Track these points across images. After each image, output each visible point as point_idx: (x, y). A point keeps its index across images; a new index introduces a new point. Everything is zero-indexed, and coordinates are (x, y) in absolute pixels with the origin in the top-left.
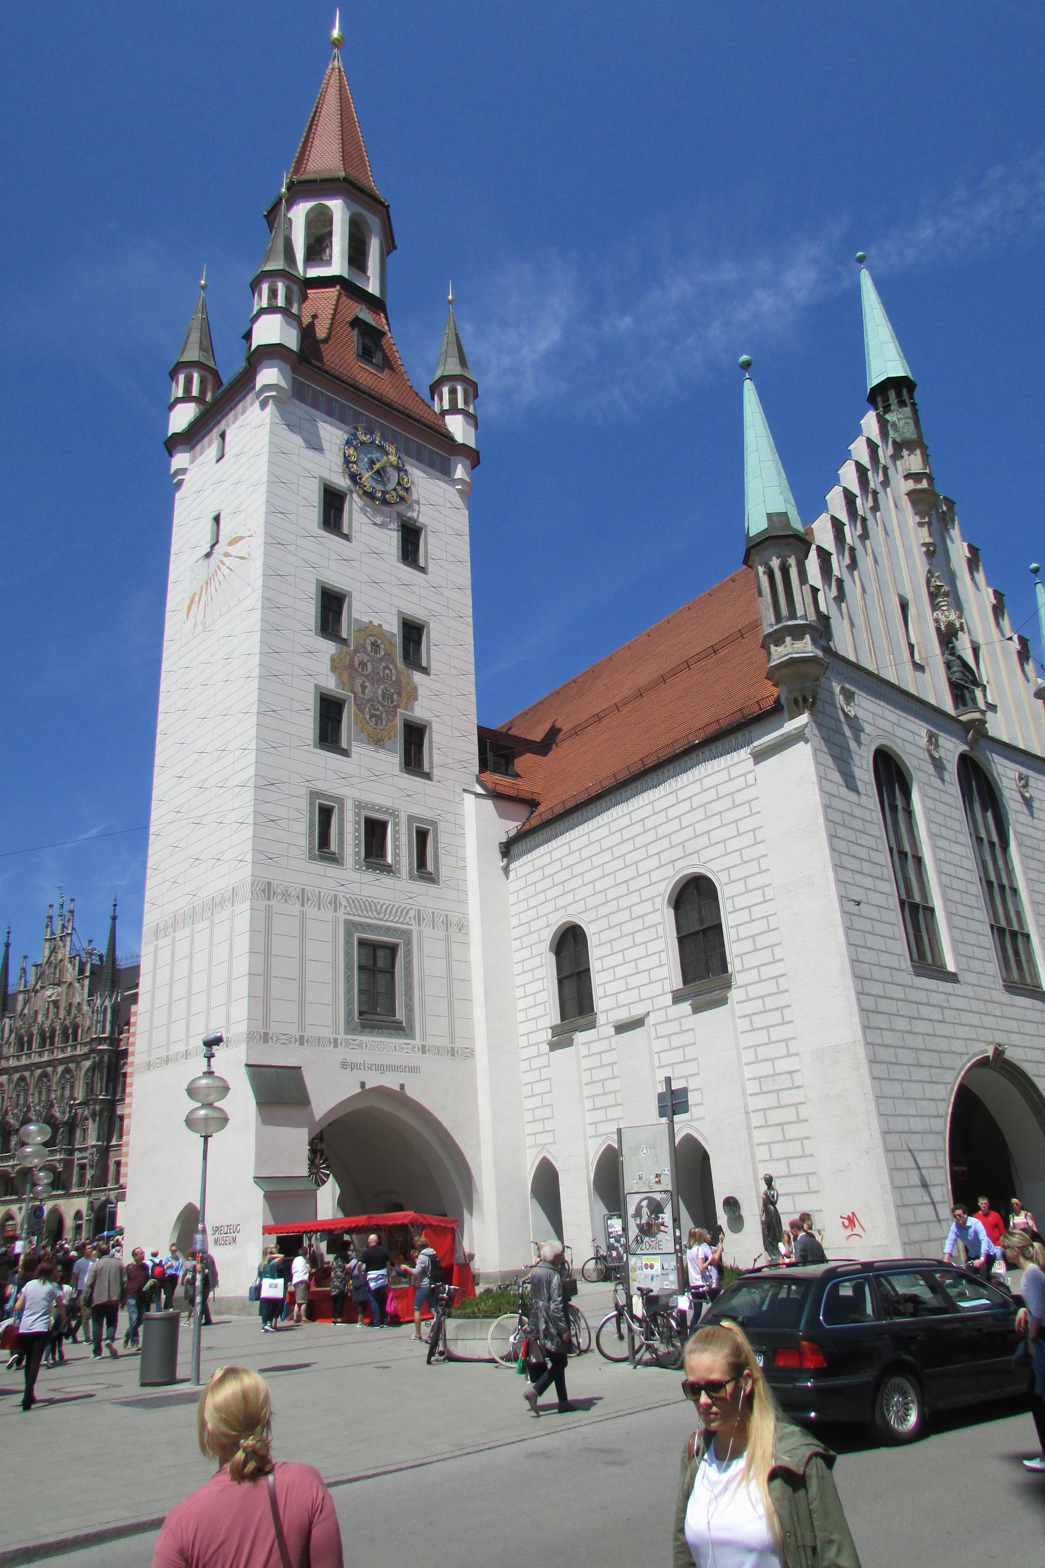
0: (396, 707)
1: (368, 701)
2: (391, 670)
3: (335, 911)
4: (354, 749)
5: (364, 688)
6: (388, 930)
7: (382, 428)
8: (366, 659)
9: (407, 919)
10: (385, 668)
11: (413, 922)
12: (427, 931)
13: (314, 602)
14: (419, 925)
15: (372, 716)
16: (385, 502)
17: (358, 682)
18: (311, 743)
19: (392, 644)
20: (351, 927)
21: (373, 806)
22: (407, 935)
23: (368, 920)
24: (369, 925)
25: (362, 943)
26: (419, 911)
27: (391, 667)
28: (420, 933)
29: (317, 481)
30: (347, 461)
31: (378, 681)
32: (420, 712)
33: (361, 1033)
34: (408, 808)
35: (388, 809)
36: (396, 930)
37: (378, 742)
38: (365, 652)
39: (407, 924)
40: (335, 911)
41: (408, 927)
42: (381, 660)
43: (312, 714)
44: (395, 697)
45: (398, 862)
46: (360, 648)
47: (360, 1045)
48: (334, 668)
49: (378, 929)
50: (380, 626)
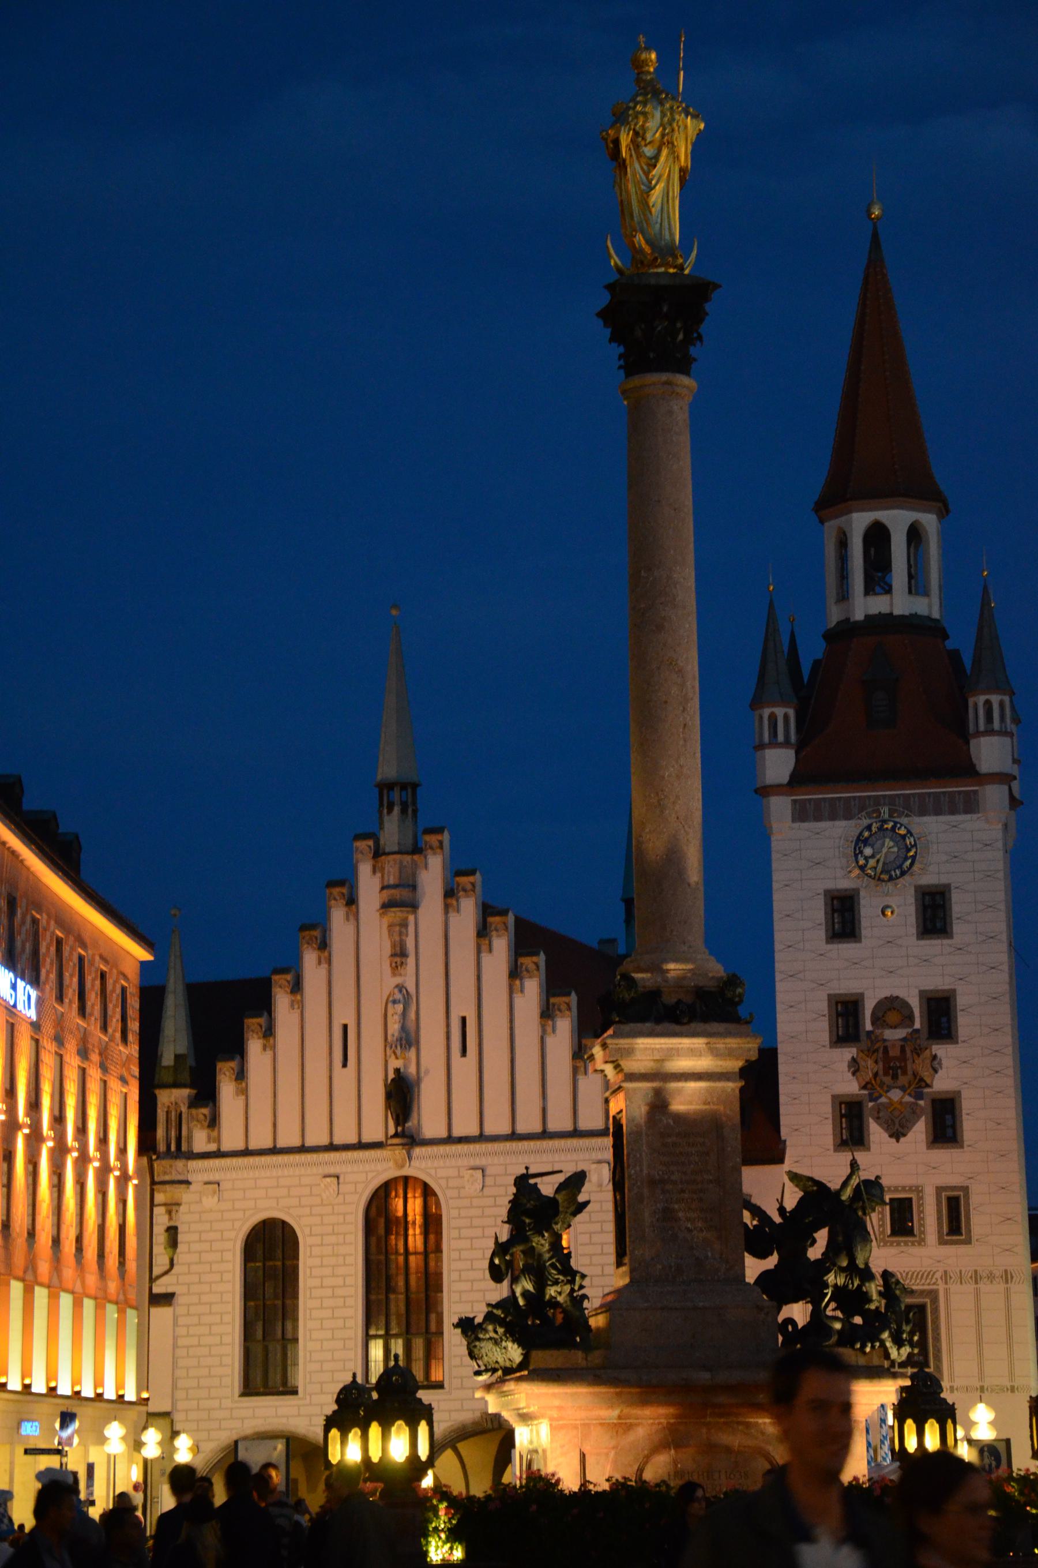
9: (934, 1280)
11: (940, 1281)
12: (954, 1287)
13: (827, 1018)
14: (946, 1283)
18: (832, 1147)
22: (933, 1295)
26: (946, 1272)
28: (947, 1291)
29: (822, 897)
32: (941, 1083)
35: (910, 1187)
39: (934, 1284)
41: (935, 1287)
43: (830, 1121)
45: (923, 1232)
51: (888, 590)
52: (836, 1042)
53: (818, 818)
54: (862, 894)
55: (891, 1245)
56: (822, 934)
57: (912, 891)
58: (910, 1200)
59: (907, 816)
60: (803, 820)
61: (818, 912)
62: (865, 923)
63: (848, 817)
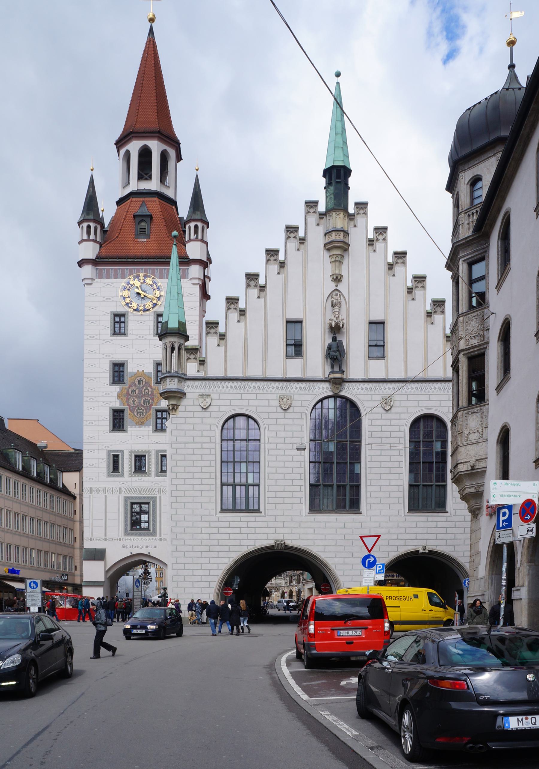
0: (151, 406)
1: (136, 407)
2: (148, 390)
3: (120, 493)
4: (129, 429)
5: (134, 402)
6: (145, 497)
7: (146, 271)
8: (135, 388)
10: (145, 390)
11: (157, 493)
13: (109, 371)
15: (138, 413)
16: (145, 310)
17: (131, 400)
19: (149, 378)
20: (126, 499)
21: (138, 451)
23: (135, 495)
24: (136, 497)
25: (132, 504)
27: (149, 388)
29: (110, 314)
30: (124, 298)
31: (142, 397)
33: (132, 535)
34: (154, 448)
35: (145, 451)
36: (148, 497)
37: (141, 423)
38: (135, 385)
40: (120, 493)
42: (143, 387)
44: (151, 401)
45: (150, 471)
46: (132, 384)
47: (131, 540)
48: (119, 397)
49: (140, 498)
50: (143, 371)
51: (150, 178)
52: (112, 383)
53: (108, 277)
54: (129, 314)
55: (135, 476)
56: (108, 331)
57: (153, 314)
58: (145, 456)
59: (153, 278)
60: (100, 277)
61: (108, 321)
62: (130, 328)
63: (123, 277)
